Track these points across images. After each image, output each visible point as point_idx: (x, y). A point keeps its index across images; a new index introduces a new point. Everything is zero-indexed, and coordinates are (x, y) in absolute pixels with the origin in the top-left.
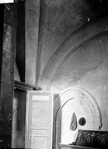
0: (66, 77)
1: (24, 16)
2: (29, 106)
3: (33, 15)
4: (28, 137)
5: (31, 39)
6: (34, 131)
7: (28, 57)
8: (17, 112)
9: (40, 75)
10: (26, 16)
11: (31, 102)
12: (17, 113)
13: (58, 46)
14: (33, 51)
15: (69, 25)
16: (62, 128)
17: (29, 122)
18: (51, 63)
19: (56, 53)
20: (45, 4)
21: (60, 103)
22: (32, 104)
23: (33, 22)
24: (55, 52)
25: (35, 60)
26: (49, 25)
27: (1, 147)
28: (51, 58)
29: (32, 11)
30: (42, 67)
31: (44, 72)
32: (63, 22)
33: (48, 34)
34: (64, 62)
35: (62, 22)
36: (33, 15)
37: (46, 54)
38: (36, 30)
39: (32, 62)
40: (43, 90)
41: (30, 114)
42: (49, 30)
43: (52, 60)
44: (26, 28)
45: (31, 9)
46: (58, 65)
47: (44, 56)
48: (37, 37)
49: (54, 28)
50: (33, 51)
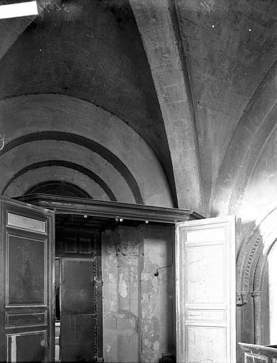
0: (272, 175)
1: (148, 66)
2: (181, 257)
3: (165, 57)
4: (182, 327)
5: (174, 106)
6: (193, 313)
7: (174, 146)
8: (165, 272)
9: (213, 180)
10: (151, 65)
11: (184, 247)
12: (168, 274)
13: (248, 102)
14: (184, 131)
15: (261, 44)
16: (270, 306)
17: (181, 295)
18: (236, 148)
19: (245, 120)
20: (190, 21)
21: (260, 239)
22: (186, 252)
23: (170, 71)
24: (241, 118)
25: (191, 149)
26: (212, 61)
27: (2, 360)
28: (234, 133)
29: (161, 50)
30: (216, 160)
31: (221, 171)
32: (244, 43)
33: (215, 82)
34: (266, 137)
35: (241, 43)
36: (165, 57)
37: (217, 129)
38: (179, 85)
39: (185, 157)
40: (221, 214)
41: (183, 276)
42: (213, 74)
43: (236, 140)
44: (158, 89)
45: (157, 47)
46: (249, 147)
47: (215, 135)
48: (185, 98)
49: (226, 64)
50: (184, 131)
